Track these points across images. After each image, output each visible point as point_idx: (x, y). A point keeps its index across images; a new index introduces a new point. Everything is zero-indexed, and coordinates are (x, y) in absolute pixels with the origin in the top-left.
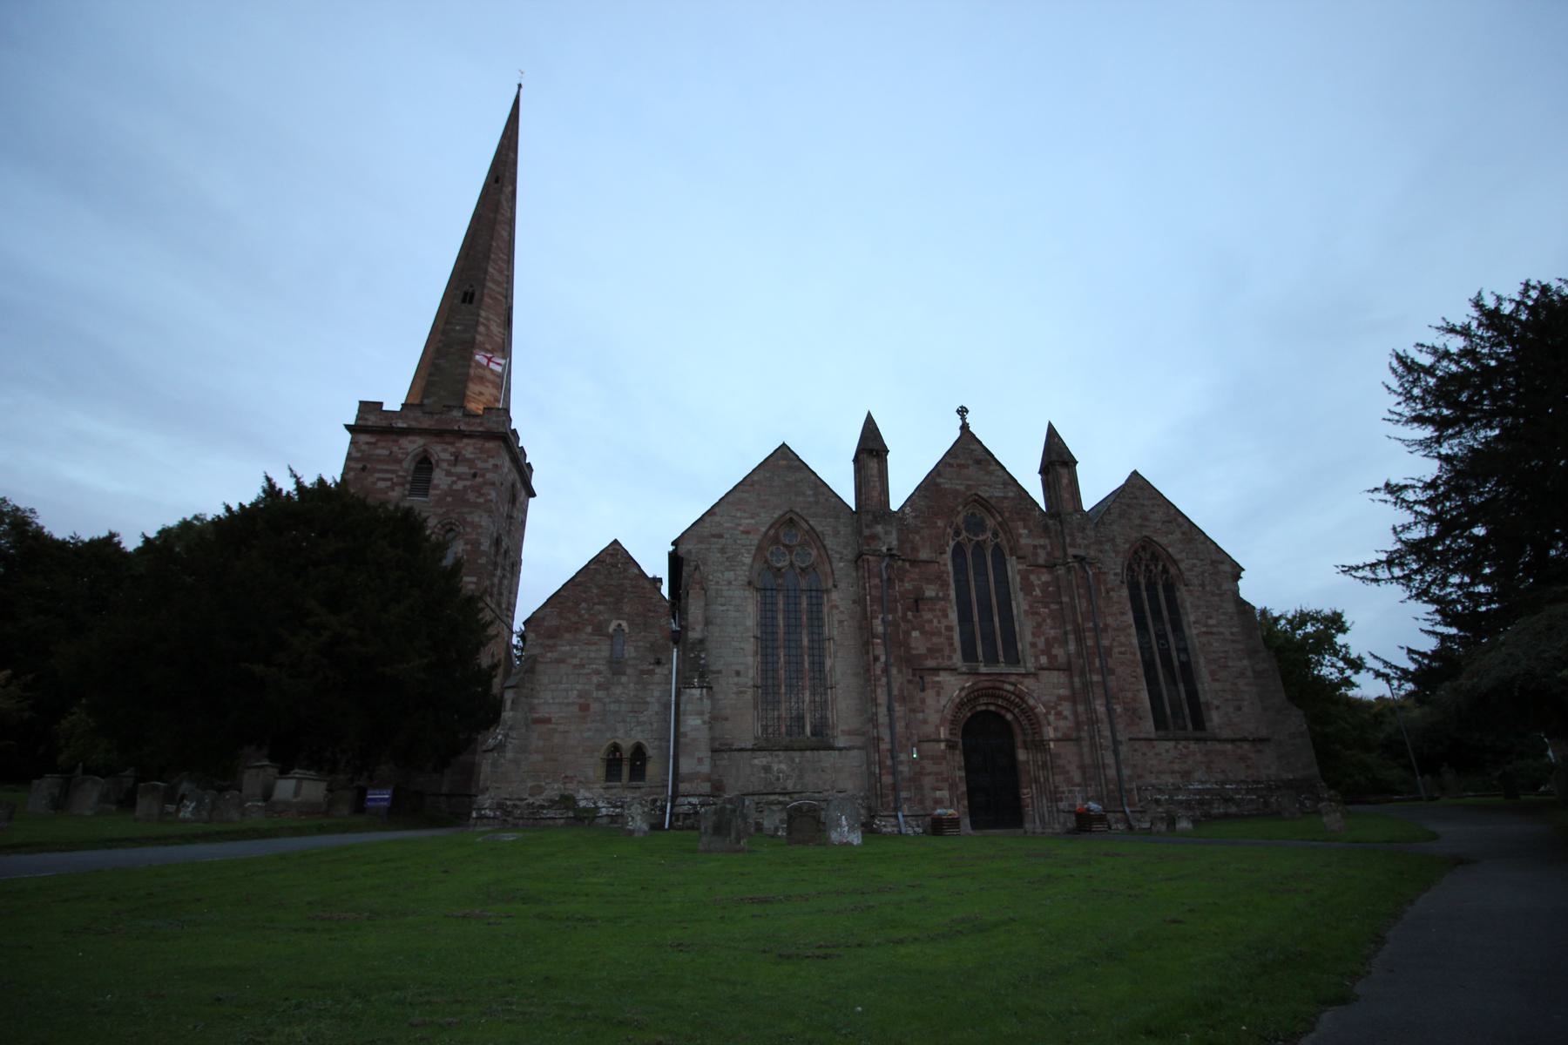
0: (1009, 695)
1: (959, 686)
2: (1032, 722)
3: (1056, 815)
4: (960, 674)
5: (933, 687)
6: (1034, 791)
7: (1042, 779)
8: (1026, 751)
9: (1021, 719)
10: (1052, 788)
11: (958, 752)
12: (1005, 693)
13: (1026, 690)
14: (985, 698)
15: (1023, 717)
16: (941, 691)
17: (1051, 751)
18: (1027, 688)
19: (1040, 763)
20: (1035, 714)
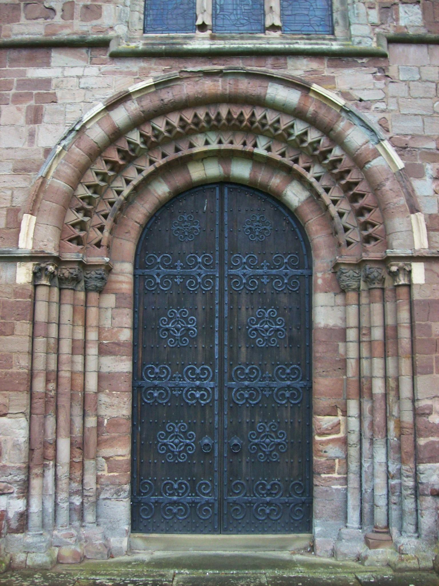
0: (285, 121)
1: (111, 93)
2: (361, 202)
3: (409, 504)
4: (116, 56)
5: (17, 99)
6: (354, 423)
7: (378, 387)
8: (339, 299)
9: (327, 198)
10: (408, 418)
11: (109, 300)
12: (272, 117)
13: (341, 102)
14: (213, 138)
15: (335, 193)
16: (47, 107)
17: (417, 296)
18: (344, 95)
19: (377, 334)
20: (369, 177)
